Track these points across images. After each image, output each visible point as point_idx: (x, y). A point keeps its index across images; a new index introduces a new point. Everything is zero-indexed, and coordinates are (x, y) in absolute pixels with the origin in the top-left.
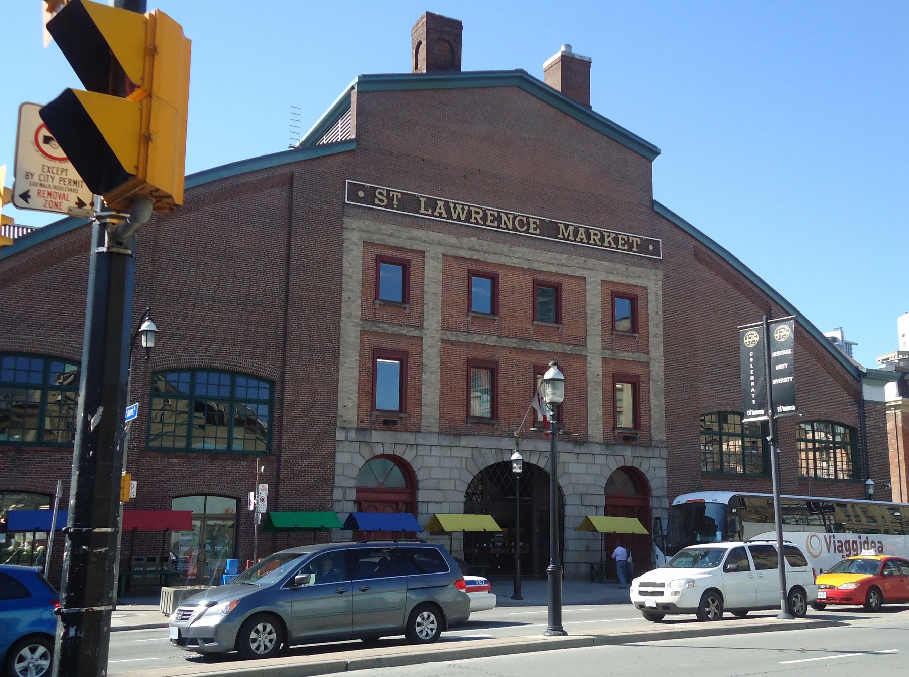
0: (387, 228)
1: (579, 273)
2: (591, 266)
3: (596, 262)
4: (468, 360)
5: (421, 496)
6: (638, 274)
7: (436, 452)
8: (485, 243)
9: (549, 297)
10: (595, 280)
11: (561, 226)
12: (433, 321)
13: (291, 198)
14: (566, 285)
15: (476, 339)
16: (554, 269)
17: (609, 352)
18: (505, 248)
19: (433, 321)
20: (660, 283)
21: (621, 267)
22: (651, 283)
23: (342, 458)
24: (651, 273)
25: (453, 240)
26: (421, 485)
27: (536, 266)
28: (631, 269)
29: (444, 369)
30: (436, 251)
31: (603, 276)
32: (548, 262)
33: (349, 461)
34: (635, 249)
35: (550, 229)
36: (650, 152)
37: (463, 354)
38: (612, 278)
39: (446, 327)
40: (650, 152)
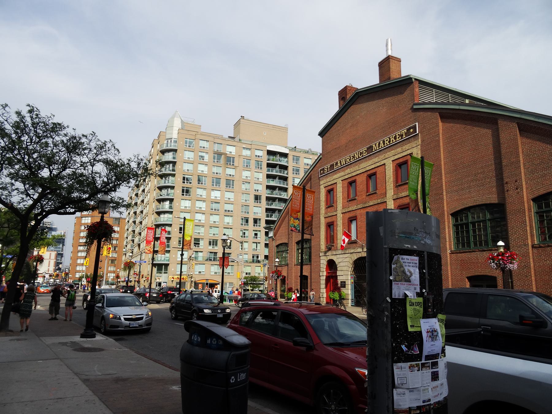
1: (382, 163)
2: (387, 156)
3: (388, 153)
4: (349, 218)
6: (407, 148)
7: (341, 256)
8: (351, 169)
11: (374, 145)
15: (350, 209)
16: (373, 166)
17: (395, 196)
18: (357, 168)
20: (419, 147)
21: (399, 150)
23: (322, 262)
24: (413, 144)
25: (342, 174)
26: (338, 269)
27: (368, 168)
28: (404, 147)
31: (393, 158)
34: (404, 136)
38: (396, 157)
39: (344, 207)
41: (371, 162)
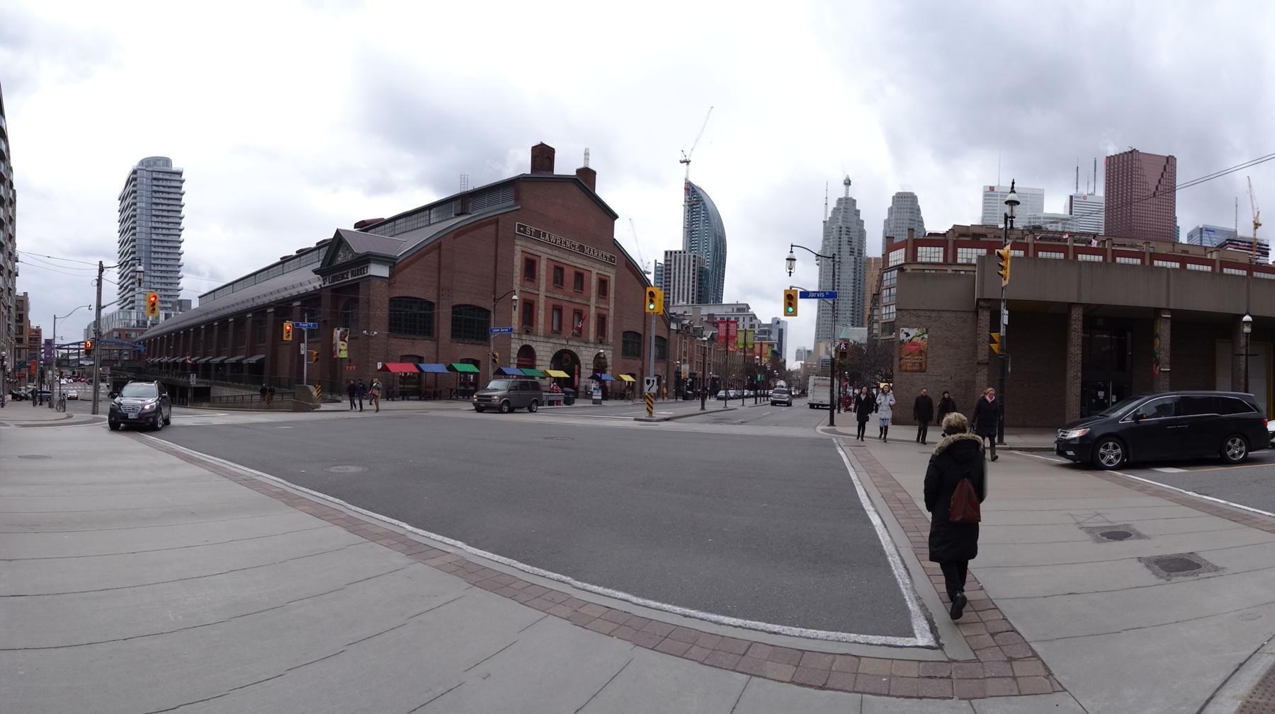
0: (530, 245)
5: (538, 363)
9: (580, 277)
10: (595, 271)
12: (543, 288)
13: (497, 230)
14: (586, 274)
19: (543, 288)
22: (611, 274)
23: (513, 345)
29: (546, 309)
30: (545, 257)
32: (580, 263)
33: (516, 346)
35: (582, 248)
36: (617, 217)
37: (552, 302)
40: (617, 217)
41: (580, 261)
